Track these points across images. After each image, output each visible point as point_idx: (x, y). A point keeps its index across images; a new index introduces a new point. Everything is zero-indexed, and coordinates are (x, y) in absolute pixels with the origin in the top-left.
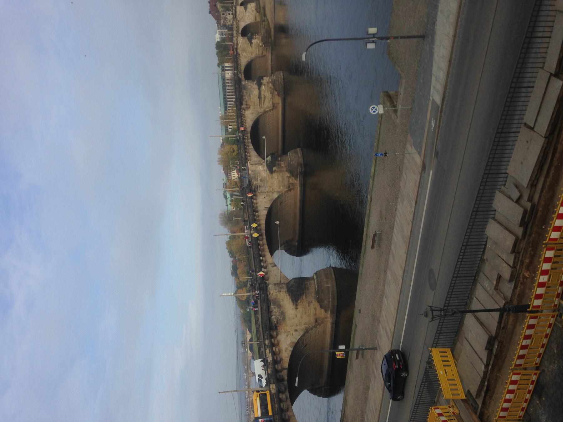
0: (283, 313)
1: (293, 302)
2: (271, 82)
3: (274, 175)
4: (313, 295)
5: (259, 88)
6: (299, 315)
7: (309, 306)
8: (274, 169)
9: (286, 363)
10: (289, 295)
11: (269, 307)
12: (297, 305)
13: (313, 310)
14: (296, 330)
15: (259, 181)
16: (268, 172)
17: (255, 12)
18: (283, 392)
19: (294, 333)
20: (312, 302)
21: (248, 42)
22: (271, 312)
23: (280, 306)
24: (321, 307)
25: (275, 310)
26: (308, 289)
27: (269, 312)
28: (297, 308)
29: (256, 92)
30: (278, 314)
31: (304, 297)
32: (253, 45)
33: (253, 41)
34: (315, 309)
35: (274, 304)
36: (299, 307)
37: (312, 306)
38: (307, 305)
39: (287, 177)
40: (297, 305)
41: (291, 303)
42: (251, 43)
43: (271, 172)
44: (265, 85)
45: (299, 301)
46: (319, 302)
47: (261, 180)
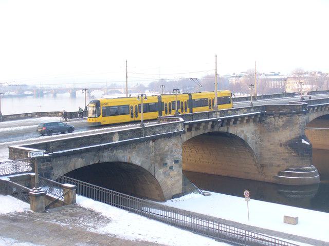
0: (277, 129)
6: (272, 147)
7: (282, 159)
9: (232, 130)
11: (285, 114)
12: (285, 145)
13: (278, 163)
14: (256, 143)
18: (212, 126)
19: (254, 140)
20: (287, 162)
22: (279, 117)
23: (284, 126)
25: (280, 122)
26: (302, 159)
27: (280, 115)
28: (281, 145)
30: (276, 124)
34: (279, 166)
35: (288, 121)
38: (283, 157)
40: (285, 145)
45: (289, 148)
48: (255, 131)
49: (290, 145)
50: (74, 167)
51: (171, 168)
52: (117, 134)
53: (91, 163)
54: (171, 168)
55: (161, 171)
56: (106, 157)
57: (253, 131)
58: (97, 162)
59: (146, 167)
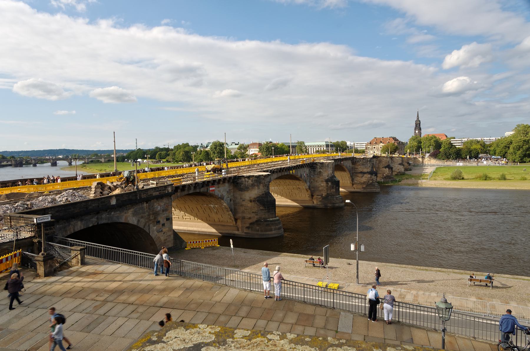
1: (257, 197)
2: (373, 182)
3: (325, 183)
4: (263, 216)
5: (368, 173)
7: (253, 212)
8: (330, 184)
10: (263, 194)
12: (254, 201)
13: (249, 216)
14: (231, 200)
15: (319, 170)
16: (327, 178)
17: (398, 171)
21: (386, 165)
24: (251, 224)
28: (251, 201)
29: (365, 170)
31: (262, 208)
32: (384, 169)
33: (387, 169)
34: (250, 218)
36: (253, 203)
37: (252, 215)
39: (322, 194)
40: (254, 201)
41: (255, 196)
42: (386, 167)
43: (327, 181)
44: (371, 177)
46: (256, 221)
47: (320, 172)
48: (230, 190)
49: (258, 201)
50: (74, 230)
51: (163, 225)
52: (114, 197)
53: (91, 225)
54: (163, 225)
55: (155, 228)
56: (104, 218)
57: (228, 190)
58: (96, 224)
59: (141, 225)
